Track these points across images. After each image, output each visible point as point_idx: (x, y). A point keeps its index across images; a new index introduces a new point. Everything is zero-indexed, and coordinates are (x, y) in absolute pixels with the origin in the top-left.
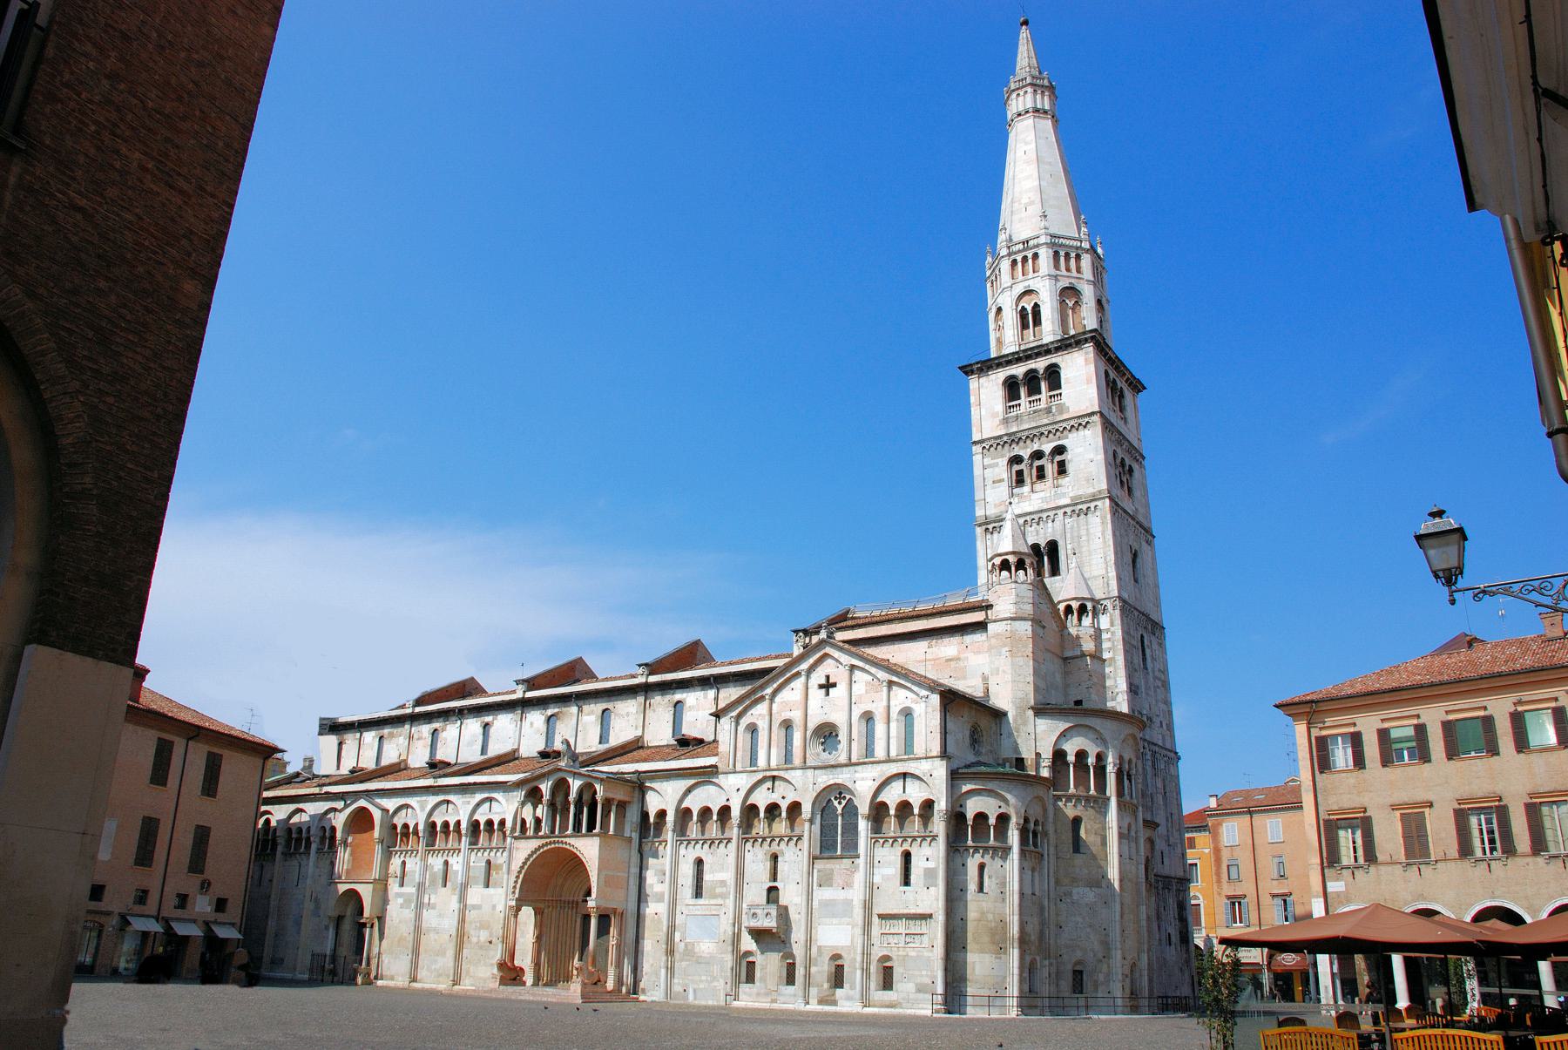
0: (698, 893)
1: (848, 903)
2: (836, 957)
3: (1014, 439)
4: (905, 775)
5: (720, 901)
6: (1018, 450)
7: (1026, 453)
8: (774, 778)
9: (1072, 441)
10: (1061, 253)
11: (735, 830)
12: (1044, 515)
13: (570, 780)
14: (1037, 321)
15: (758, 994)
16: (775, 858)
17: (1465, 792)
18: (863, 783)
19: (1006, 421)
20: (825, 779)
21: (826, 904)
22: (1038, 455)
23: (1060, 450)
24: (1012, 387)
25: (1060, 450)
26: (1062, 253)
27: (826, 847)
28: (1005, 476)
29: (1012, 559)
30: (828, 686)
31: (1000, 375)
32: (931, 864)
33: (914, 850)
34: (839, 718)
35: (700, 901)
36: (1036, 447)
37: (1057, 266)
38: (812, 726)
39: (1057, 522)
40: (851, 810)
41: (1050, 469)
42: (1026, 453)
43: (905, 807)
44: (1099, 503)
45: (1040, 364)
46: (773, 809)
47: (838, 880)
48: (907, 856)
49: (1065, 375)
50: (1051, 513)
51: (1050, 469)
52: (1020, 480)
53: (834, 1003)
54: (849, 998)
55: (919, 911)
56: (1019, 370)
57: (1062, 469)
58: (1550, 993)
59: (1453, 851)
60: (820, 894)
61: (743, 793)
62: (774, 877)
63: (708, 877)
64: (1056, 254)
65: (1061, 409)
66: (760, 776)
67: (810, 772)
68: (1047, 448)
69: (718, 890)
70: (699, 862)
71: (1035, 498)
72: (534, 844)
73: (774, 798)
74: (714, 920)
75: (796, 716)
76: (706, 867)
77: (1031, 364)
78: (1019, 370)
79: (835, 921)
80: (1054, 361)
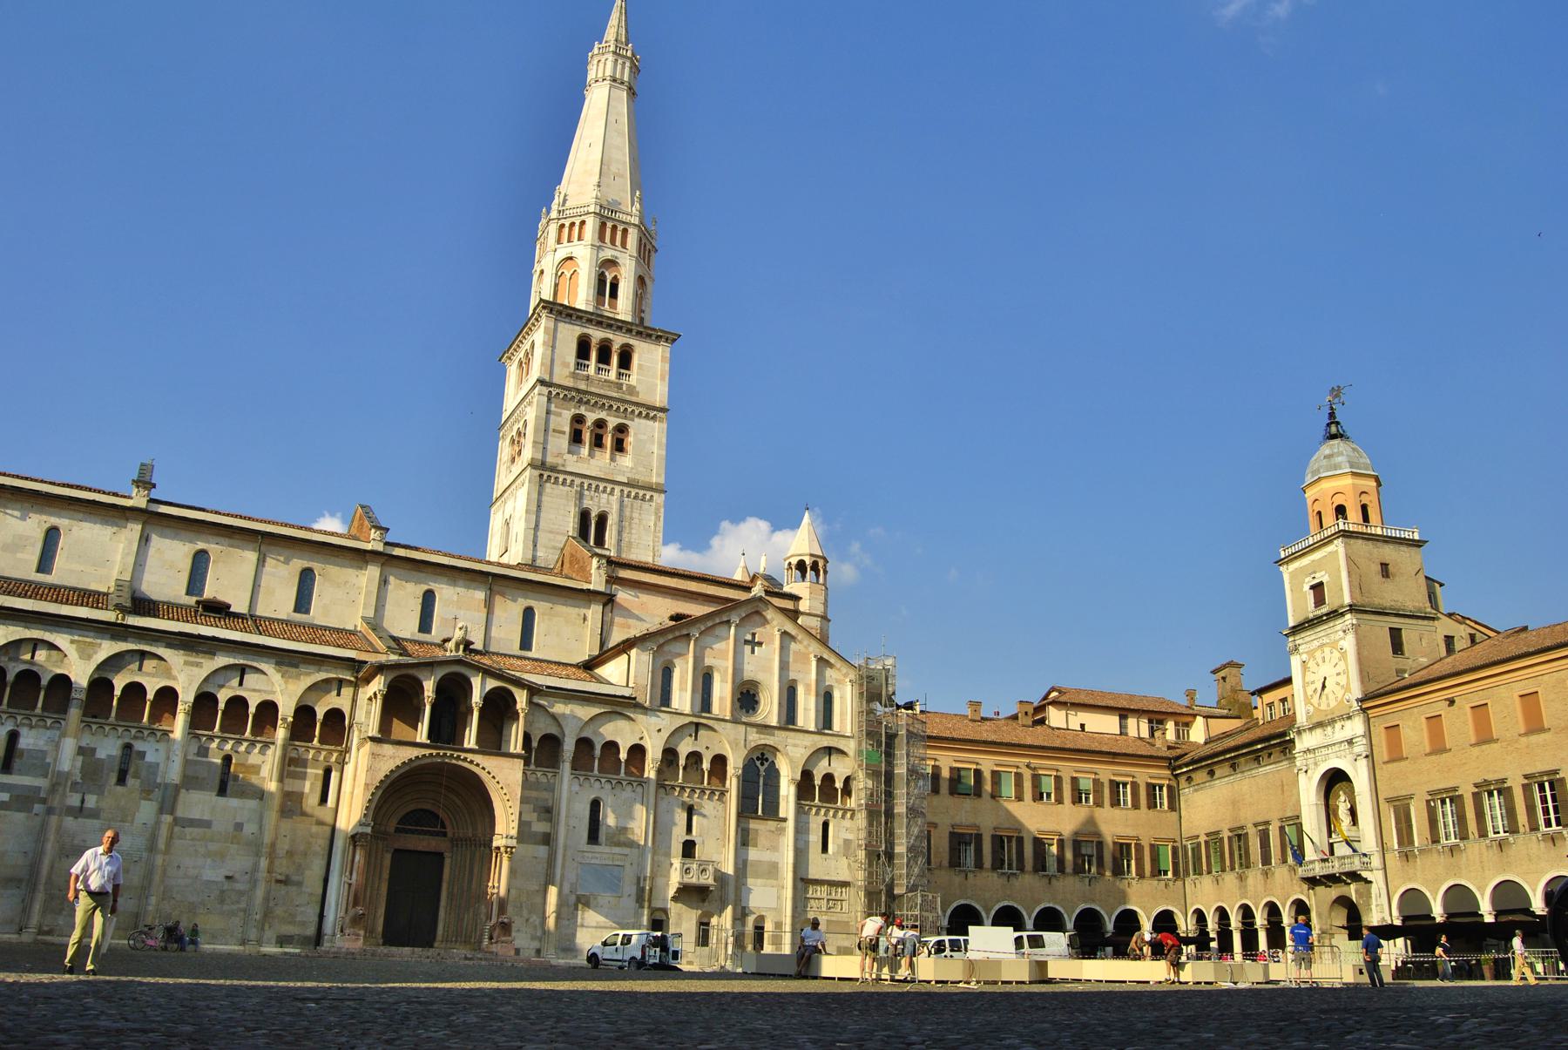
0: (593, 837)
4: (829, 751)
6: (582, 410)
7: (591, 417)
8: (697, 725)
10: (608, 224)
14: (614, 295)
17: (957, 820)
19: (574, 375)
20: (756, 738)
22: (600, 424)
25: (622, 429)
26: (609, 225)
27: (746, 809)
28: (567, 429)
29: (808, 561)
30: (754, 644)
35: (596, 848)
36: (602, 415)
37: (602, 238)
40: (773, 774)
41: (608, 440)
42: (591, 417)
44: (656, 495)
49: (636, 360)
51: (608, 440)
52: (576, 438)
56: (597, 334)
57: (619, 446)
58: (1177, 966)
59: (946, 863)
61: (665, 735)
62: (689, 829)
64: (603, 225)
67: (742, 728)
68: (612, 422)
70: (595, 805)
71: (599, 463)
80: (611, 336)
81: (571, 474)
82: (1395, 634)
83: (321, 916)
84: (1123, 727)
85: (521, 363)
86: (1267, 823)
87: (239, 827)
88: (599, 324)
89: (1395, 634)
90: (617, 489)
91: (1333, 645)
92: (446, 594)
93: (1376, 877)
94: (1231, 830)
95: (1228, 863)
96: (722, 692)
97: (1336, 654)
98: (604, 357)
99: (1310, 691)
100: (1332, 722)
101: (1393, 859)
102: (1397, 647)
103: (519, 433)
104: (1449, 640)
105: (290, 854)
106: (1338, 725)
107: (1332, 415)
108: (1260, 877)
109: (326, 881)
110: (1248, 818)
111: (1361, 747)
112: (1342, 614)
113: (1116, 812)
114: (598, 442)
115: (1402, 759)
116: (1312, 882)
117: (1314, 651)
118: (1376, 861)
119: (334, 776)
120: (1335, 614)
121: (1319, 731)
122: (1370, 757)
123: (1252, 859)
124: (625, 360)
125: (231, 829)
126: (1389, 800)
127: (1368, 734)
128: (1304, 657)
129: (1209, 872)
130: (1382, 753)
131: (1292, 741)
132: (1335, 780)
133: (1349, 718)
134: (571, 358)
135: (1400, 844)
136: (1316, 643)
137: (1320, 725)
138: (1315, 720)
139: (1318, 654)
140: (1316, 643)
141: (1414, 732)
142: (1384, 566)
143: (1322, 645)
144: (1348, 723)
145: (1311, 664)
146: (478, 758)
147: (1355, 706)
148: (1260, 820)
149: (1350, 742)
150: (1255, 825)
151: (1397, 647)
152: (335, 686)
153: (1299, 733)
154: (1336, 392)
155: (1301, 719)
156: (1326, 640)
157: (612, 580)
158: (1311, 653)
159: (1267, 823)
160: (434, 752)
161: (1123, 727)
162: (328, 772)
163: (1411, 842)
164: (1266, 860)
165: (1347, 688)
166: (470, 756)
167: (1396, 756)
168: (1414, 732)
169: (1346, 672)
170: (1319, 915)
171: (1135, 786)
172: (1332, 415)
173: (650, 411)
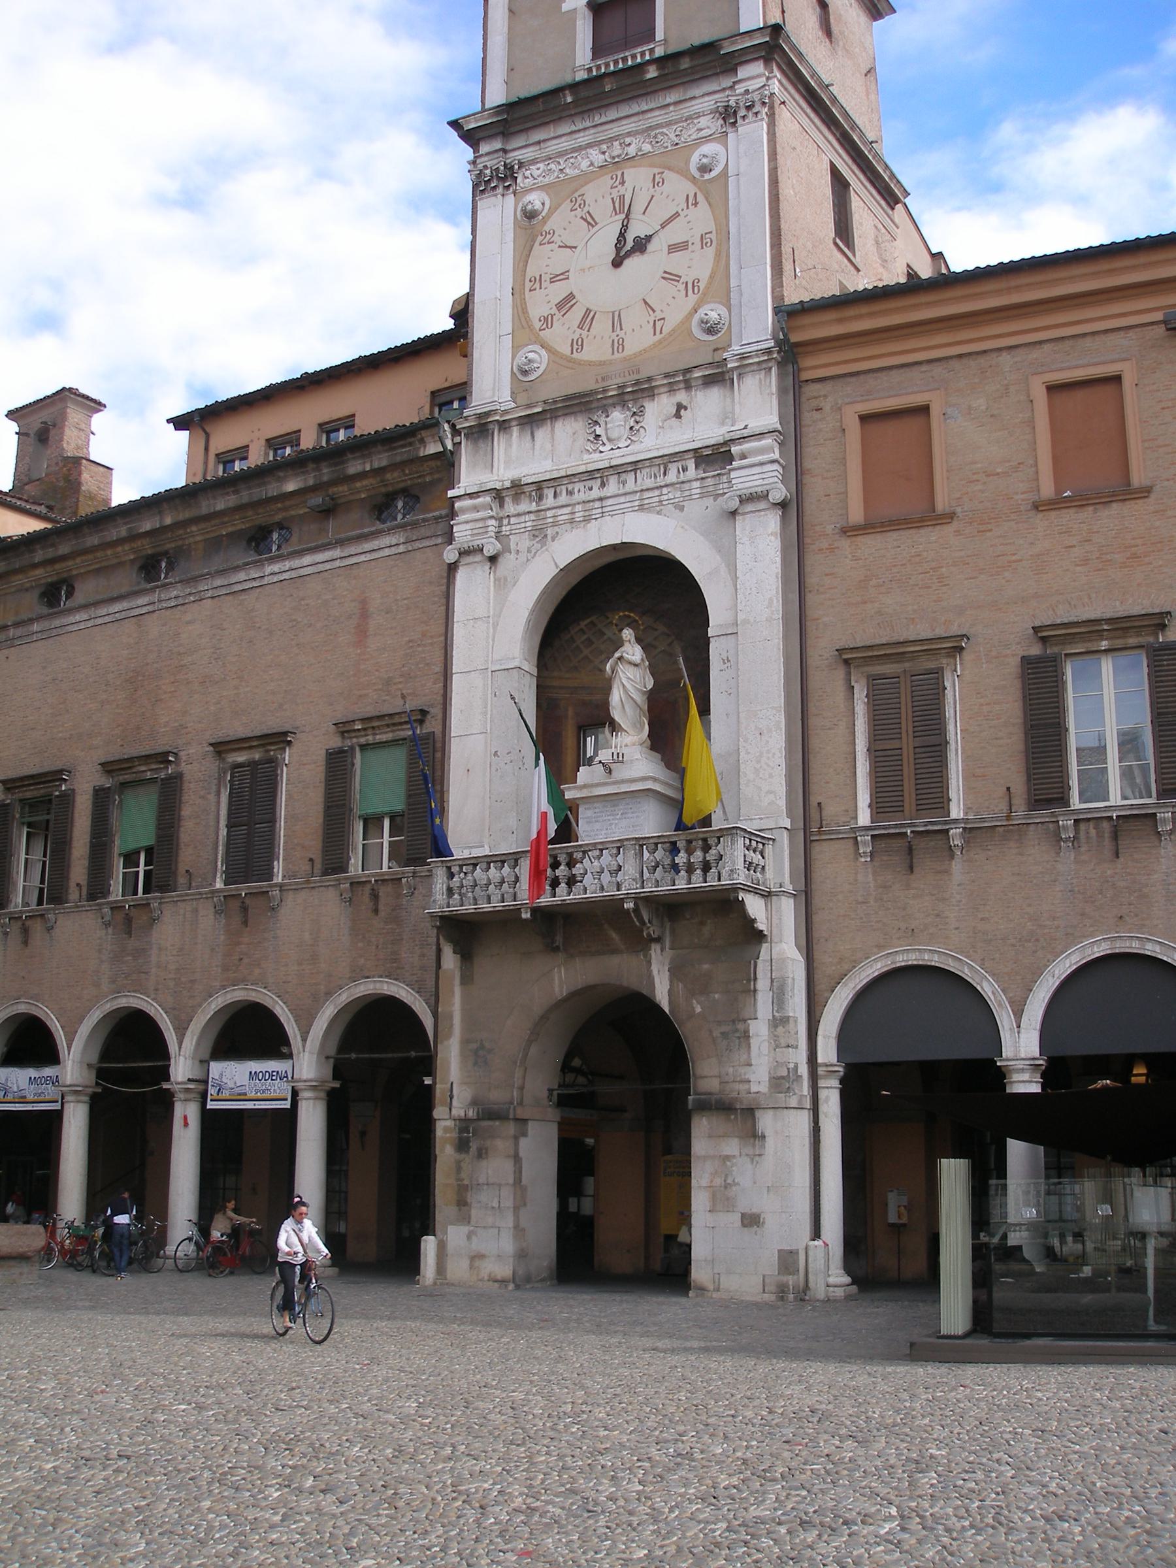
86: (281, 738)
91: (671, 160)
93: (777, 919)
94: (108, 767)
95: (79, 872)
97: (677, 187)
99: (540, 304)
100: (635, 394)
101: (845, 873)
106: (657, 408)
108: (207, 919)
110: (191, 724)
111: (762, 471)
115: (932, 517)
116: (465, 932)
117: (585, 178)
118: (779, 867)
120: (709, 60)
122: (792, 508)
123: (187, 857)
126: (848, 659)
127: (794, 436)
128: (535, 200)
130: (842, 489)
131: (447, 463)
133: (710, 381)
135: (878, 807)
136: (596, 156)
137: (582, 405)
138: (554, 390)
140: (596, 156)
141: (989, 428)
143: (617, 164)
144: (707, 402)
145: (564, 223)
147: (757, 328)
149: (716, 457)
150: (221, 748)
158: (567, 191)
159: (281, 738)
163: (934, 795)
164: (250, 853)
165: (720, 286)
167: (904, 498)
168: (989, 428)
169: (720, 240)
170: (476, 1054)
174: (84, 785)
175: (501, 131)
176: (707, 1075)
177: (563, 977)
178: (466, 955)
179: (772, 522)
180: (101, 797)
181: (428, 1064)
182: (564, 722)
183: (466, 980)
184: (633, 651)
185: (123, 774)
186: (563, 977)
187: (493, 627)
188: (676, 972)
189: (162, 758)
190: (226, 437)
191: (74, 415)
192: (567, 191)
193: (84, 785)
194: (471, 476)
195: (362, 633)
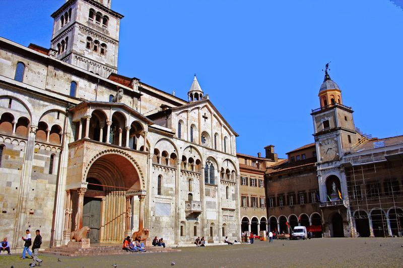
0: (159, 193)
1: (215, 203)
2: (212, 224)
3: (90, 31)
5: (171, 197)
6: (90, 36)
7: (94, 39)
9: (108, 44)
11: (180, 165)
12: (97, 64)
13: (127, 116)
15: (187, 241)
16: (190, 180)
18: (220, 158)
21: (208, 203)
22: (97, 42)
23: (104, 45)
24: (92, 13)
31: (90, 6)
32: (234, 193)
33: (229, 186)
34: (210, 133)
35: (162, 197)
36: (97, 39)
38: (201, 131)
39: (100, 69)
41: (99, 49)
42: (94, 39)
43: (228, 171)
45: (104, 13)
46: (191, 160)
47: (211, 193)
48: (227, 187)
50: (100, 65)
51: (99, 49)
52: (88, 46)
53: (212, 242)
54: (217, 240)
55: (232, 208)
56: (97, 10)
57: (102, 52)
60: (207, 199)
61: (183, 149)
63: (165, 185)
65: (107, 32)
66: (189, 145)
68: (101, 42)
69: (170, 192)
70: (160, 176)
72: (102, 148)
73: (192, 156)
74: (168, 206)
75: (197, 124)
76: (163, 180)
77: (100, 11)
78: (97, 10)
79: (212, 210)
81: (87, 58)
82: (349, 136)
83: (53, 231)
84: (246, 162)
85: (62, 17)
87: (9, 184)
88: (97, 6)
89: (349, 136)
90: (103, 66)
91: (332, 139)
92: (82, 83)
96: (197, 135)
98: (98, 19)
102: (350, 141)
103: (63, 42)
104: (359, 139)
105: (36, 199)
106: (334, 163)
107: (326, 73)
109: (54, 212)
110: (296, 189)
112: (337, 130)
113: (251, 187)
114: (95, 49)
119: (56, 159)
121: (326, 164)
124: (106, 20)
125: (5, 185)
129: (278, 205)
132: (332, 180)
134: (87, 16)
139: (326, 142)
142: (345, 117)
143: (328, 139)
146: (130, 153)
148: (300, 190)
151: (350, 141)
152: (56, 114)
153: (319, 164)
154: (327, 66)
155: (319, 161)
156: (329, 137)
157: (140, 89)
158: (323, 141)
160: (113, 149)
161: (246, 162)
162: (52, 156)
166: (127, 152)
170: (325, 219)
171: (256, 180)
172: (326, 73)
173: (113, 41)
174: (286, 195)
175: (317, 135)
176: (344, 220)
177: (332, 212)
178: (323, 210)
179: (344, 173)
180: (287, 196)
181: (321, 219)
182: (329, 191)
183: (323, 212)
184: (334, 184)
185: (289, 195)
186: (332, 212)
187: (322, 180)
188: (340, 211)
189: (293, 192)
190: (292, 155)
191: (272, 148)
192: (323, 141)
193: (286, 195)
194: (318, 169)
195: (310, 182)
